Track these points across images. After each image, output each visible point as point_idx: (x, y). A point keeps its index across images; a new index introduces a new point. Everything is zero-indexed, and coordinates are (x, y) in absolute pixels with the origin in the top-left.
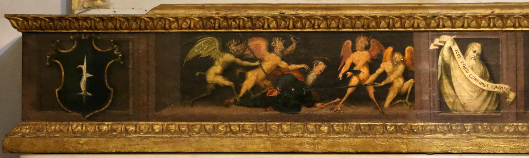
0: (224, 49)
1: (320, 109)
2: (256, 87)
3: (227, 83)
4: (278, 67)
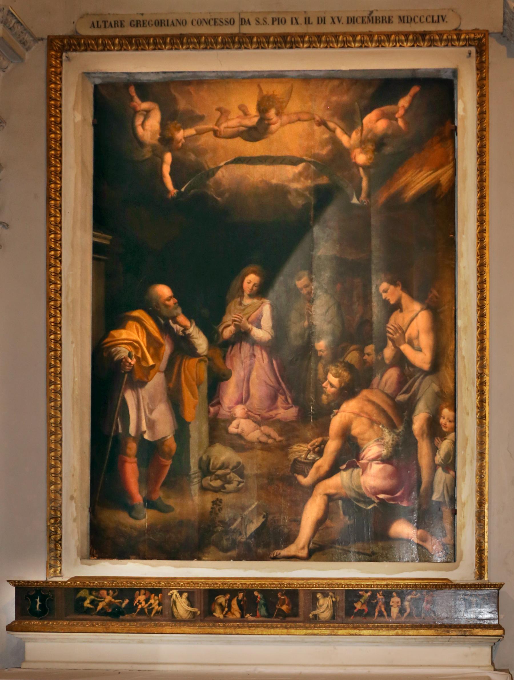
0: (91, 594)
1: (127, 617)
2: (102, 609)
3: (91, 607)
4: (111, 601)
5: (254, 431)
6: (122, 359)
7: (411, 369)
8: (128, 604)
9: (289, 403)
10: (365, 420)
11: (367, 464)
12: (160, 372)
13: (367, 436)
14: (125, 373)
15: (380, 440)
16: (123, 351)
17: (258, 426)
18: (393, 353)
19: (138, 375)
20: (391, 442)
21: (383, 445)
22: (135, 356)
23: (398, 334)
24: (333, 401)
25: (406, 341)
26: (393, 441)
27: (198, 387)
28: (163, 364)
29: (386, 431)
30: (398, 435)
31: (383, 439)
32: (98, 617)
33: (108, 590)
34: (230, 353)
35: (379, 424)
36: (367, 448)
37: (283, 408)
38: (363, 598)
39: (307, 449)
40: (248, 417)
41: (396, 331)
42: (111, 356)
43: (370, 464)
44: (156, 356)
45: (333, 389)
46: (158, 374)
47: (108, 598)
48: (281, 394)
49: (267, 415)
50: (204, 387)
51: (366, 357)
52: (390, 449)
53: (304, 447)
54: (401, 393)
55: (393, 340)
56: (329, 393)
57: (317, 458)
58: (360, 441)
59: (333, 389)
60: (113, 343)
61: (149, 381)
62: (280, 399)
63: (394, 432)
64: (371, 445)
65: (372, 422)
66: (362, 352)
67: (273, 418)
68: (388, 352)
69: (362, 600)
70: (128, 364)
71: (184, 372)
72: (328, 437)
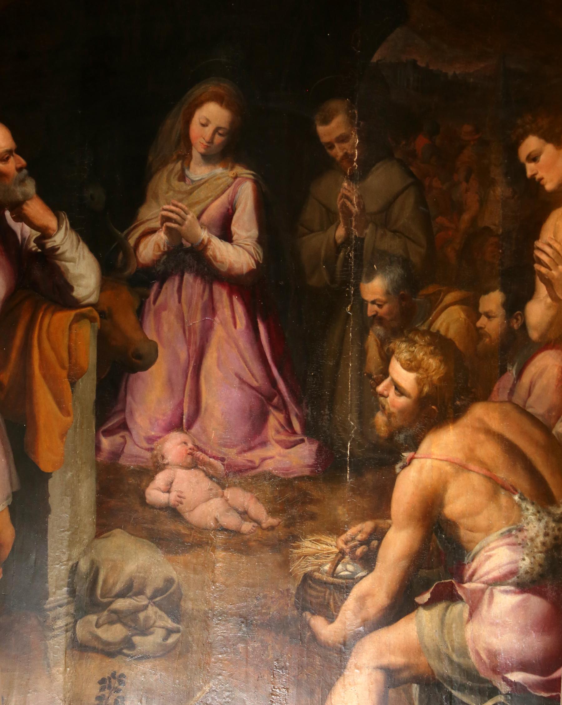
9: (294, 433)
11: (483, 591)
17: (217, 489)
20: (541, 538)
21: (522, 545)
24: (400, 430)
26: (546, 535)
29: (530, 510)
35: (511, 490)
37: (278, 442)
39: (337, 550)
43: (488, 592)
45: (402, 401)
48: (276, 408)
49: (242, 459)
51: (483, 322)
52: (540, 556)
55: (549, 283)
56: (392, 410)
58: (464, 534)
59: (402, 401)
63: (549, 514)
64: (492, 545)
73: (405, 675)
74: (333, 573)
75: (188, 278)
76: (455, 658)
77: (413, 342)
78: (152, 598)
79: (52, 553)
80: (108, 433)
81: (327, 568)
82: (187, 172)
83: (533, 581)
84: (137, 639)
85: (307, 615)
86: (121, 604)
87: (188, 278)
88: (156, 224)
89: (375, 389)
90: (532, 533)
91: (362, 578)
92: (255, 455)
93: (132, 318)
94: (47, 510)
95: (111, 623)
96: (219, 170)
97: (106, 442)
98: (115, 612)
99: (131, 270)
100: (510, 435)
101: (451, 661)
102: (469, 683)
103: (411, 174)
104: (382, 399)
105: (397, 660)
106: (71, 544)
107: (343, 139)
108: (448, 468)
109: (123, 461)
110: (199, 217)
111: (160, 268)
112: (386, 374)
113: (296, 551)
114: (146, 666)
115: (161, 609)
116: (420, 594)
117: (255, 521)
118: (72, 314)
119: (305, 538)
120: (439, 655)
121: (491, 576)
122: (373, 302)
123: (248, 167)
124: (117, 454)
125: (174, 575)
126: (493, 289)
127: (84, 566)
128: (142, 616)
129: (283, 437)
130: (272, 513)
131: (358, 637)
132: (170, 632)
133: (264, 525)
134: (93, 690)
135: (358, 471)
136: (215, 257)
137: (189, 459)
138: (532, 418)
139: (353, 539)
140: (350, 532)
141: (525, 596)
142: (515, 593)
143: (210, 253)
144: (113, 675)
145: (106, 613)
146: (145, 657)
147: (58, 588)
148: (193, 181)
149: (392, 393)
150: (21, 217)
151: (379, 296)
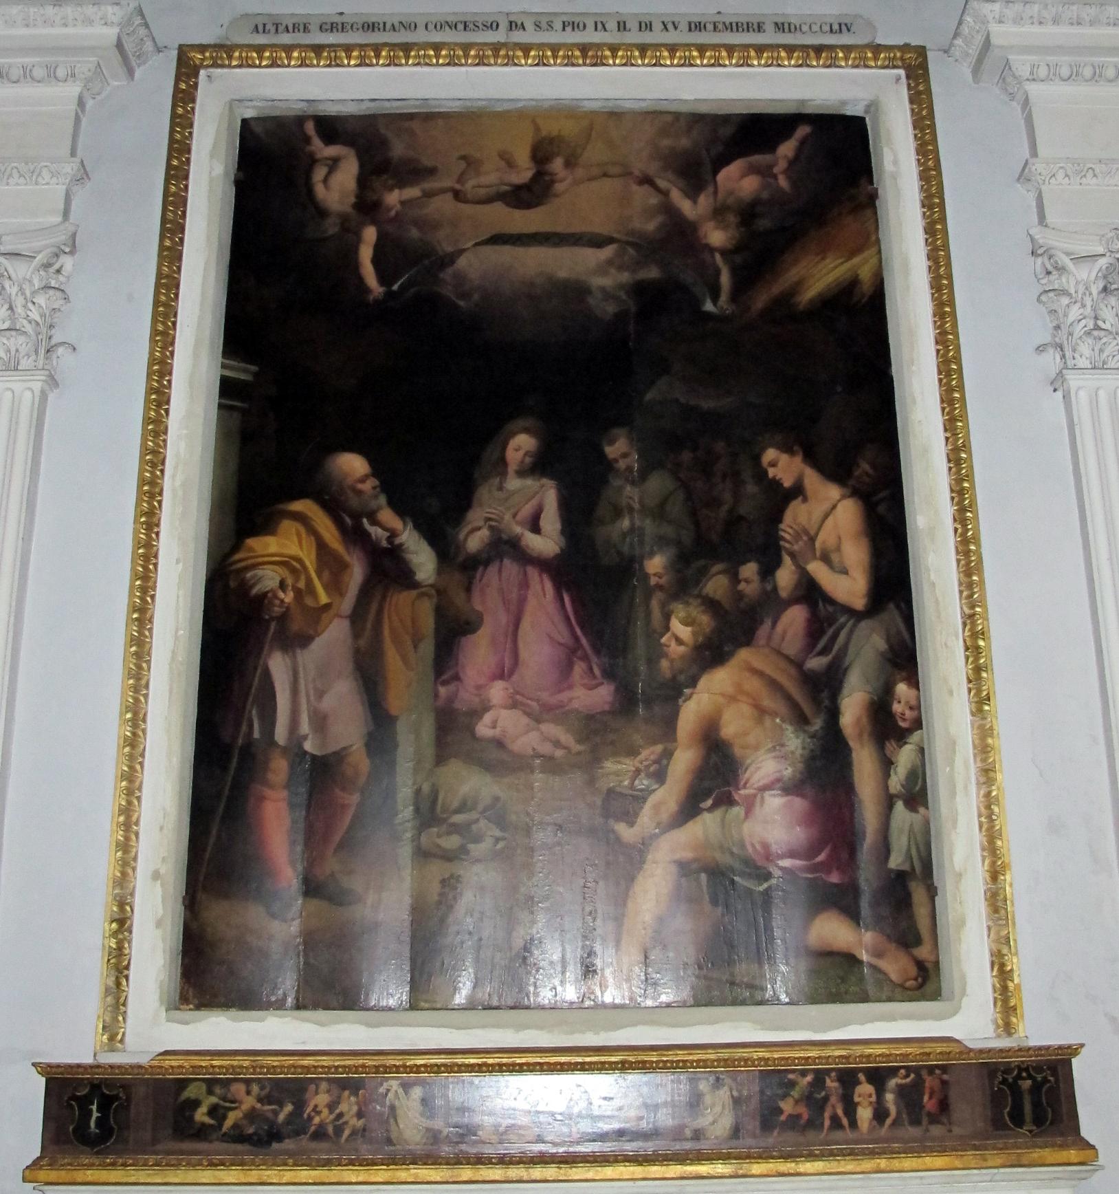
0: (210, 1092)
1: (288, 1144)
2: (235, 1126)
3: (212, 1122)
4: (253, 1109)
5: (527, 732)
6: (267, 592)
7: (830, 609)
8: (291, 1114)
9: (594, 677)
10: (746, 709)
11: (755, 796)
12: (341, 617)
13: (751, 739)
14: (272, 619)
15: (778, 748)
16: (268, 579)
17: (533, 724)
18: (796, 577)
19: (297, 624)
20: (799, 751)
21: (784, 757)
22: (293, 586)
23: (800, 543)
24: (681, 672)
25: (818, 554)
26: (804, 748)
27: (415, 647)
28: (347, 603)
29: (789, 730)
30: (813, 736)
31: (783, 745)
32: (225, 1145)
33: (248, 1082)
34: (480, 581)
35: (774, 714)
36: (754, 765)
37: (584, 685)
38: (797, 1088)
39: (634, 769)
40: (514, 705)
41: (797, 536)
42: (244, 587)
43: (759, 796)
44: (336, 586)
45: (682, 649)
46: (336, 622)
47: (249, 1102)
48: (581, 659)
49: (553, 700)
50: (428, 648)
51: (742, 586)
52: (800, 766)
53: (627, 765)
54: (814, 653)
55: (793, 555)
56: (673, 656)
57: (655, 787)
58: (737, 751)
59: (682, 649)
60: (250, 562)
61: (318, 636)
62: (579, 668)
63: (805, 731)
64: (760, 759)
65: (761, 712)
66: (735, 579)
67: (562, 707)
68: (785, 577)
69: (795, 1093)
70: (277, 602)
71: (389, 618)
72: (674, 744)
73: (694, 866)
74: (632, 786)
75: (507, 562)
76: (735, 850)
77: (687, 604)
78: (484, 811)
79: (399, 779)
80: (445, 683)
81: (626, 783)
82: (504, 485)
83: (795, 786)
84: (471, 846)
85: (611, 822)
86: (458, 818)
87: (507, 562)
88: (481, 523)
89: (659, 641)
90: (792, 748)
91: (654, 790)
92: (564, 696)
93: (463, 595)
94: (396, 746)
95: (449, 833)
96: (529, 482)
97: (443, 691)
98: (454, 825)
99: (461, 559)
100: (769, 670)
101: (732, 853)
102: (748, 870)
103: (679, 479)
104: (665, 648)
105: (688, 855)
106: (416, 771)
107: (625, 455)
108: (721, 700)
109: (457, 705)
110: (514, 516)
111: (484, 556)
112: (667, 628)
113: (600, 771)
114: (477, 868)
115: (490, 821)
116: (704, 800)
117: (565, 748)
118: (414, 593)
119: (607, 760)
120: (721, 847)
121: (761, 784)
122: (655, 575)
123: (552, 479)
124: (451, 699)
125: (501, 794)
126: (749, 561)
127: (426, 788)
128: (474, 827)
129: (586, 681)
130: (579, 742)
131: (654, 837)
132: (497, 840)
133: (573, 752)
134: (435, 887)
135: (649, 703)
136: (527, 546)
137: (510, 701)
138: (787, 657)
139: (646, 760)
140: (645, 753)
141: (790, 798)
142: (782, 796)
143: (523, 543)
144: (452, 876)
145: (445, 826)
146: (478, 861)
147: (405, 807)
148: (507, 490)
149: (673, 644)
150: (375, 522)
151: (660, 570)
